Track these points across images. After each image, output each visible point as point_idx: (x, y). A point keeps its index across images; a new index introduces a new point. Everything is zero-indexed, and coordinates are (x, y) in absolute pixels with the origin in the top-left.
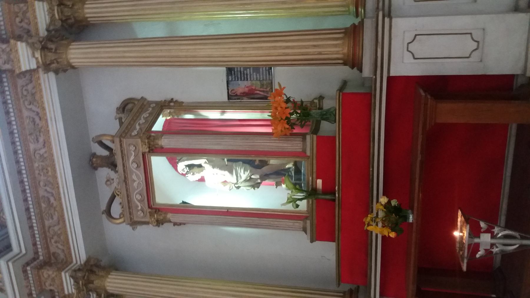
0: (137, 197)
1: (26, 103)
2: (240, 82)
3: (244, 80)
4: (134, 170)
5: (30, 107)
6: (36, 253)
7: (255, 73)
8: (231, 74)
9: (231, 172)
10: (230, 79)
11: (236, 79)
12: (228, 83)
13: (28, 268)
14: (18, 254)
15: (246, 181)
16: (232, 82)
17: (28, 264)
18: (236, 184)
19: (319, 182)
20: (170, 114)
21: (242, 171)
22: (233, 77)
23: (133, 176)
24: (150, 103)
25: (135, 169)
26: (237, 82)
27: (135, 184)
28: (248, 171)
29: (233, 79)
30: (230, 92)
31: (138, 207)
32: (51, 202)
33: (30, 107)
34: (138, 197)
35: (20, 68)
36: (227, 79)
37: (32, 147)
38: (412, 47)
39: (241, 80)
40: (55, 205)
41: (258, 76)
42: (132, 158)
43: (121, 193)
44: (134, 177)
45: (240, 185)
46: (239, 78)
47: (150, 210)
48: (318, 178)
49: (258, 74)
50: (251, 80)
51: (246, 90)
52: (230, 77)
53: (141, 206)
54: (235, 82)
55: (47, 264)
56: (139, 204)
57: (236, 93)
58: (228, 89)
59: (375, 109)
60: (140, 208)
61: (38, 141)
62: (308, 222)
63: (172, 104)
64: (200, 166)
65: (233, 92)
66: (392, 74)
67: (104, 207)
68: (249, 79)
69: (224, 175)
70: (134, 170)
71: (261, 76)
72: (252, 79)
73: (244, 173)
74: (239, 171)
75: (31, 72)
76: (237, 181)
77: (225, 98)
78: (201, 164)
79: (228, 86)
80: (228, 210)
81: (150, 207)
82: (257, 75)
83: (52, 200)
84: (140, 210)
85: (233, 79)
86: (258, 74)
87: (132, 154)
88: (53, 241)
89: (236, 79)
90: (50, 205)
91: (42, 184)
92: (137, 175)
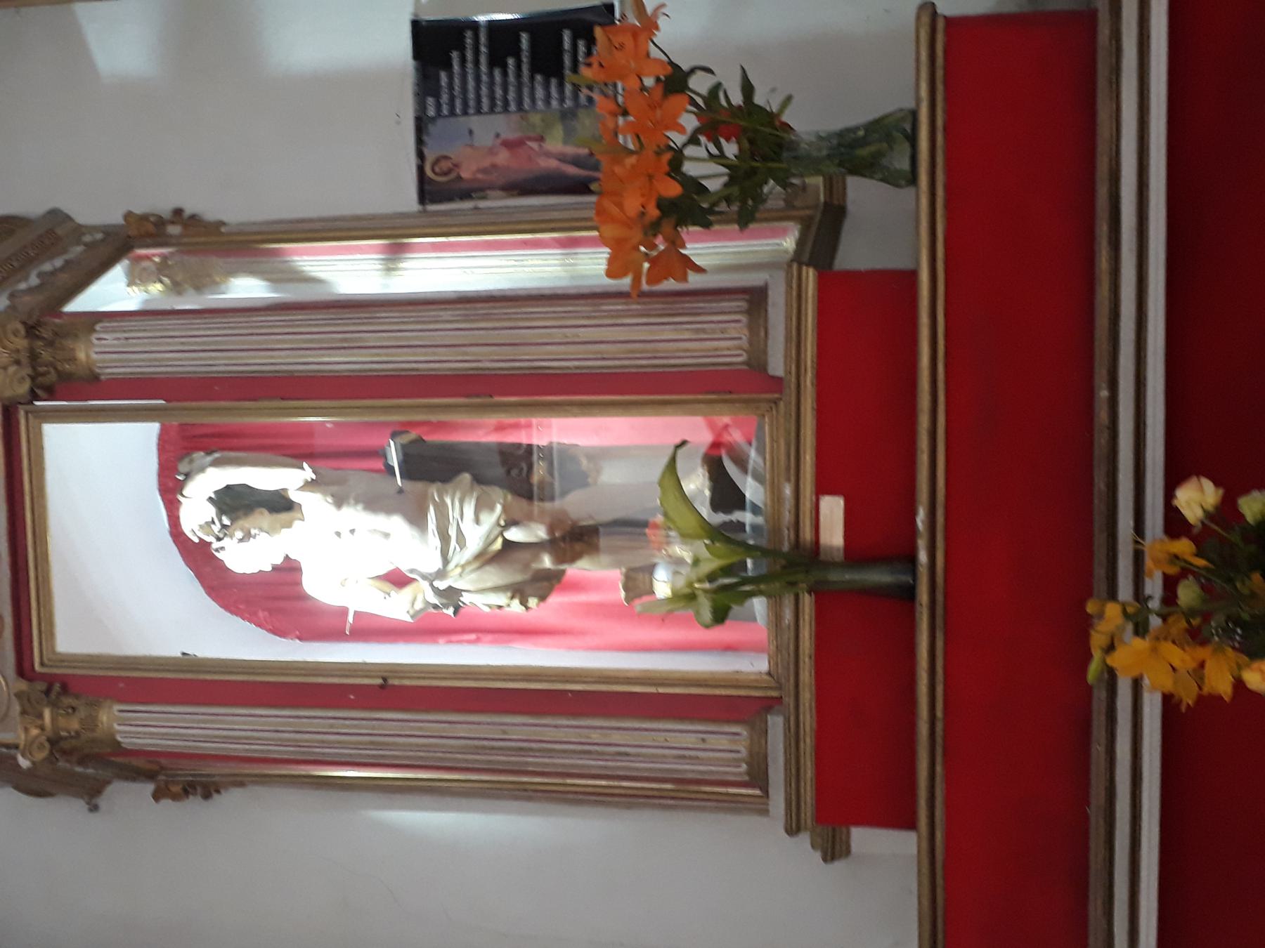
2: (474, 122)
3: (492, 109)
7: (539, 78)
8: (437, 96)
9: (417, 519)
10: (431, 112)
11: (458, 103)
12: (421, 125)
15: (485, 559)
16: (440, 122)
18: (441, 574)
19: (833, 509)
21: (469, 509)
22: (445, 98)
24: (79, 231)
26: (462, 119)
28: (492, 509)
29: (445, 111)
36: (416, 111)
39: (479, 111)
45: (458, 585)
46: (472, 103)
47: (23, 685)
48: (823, 488)
54: (452, 120)
57: (452, 176)
58: (421, 155)
59: (1117, 70)
62: (776, 723)
64: (280, 504)
65: (445, 165)
68: (513, 107)
69: (387, 535)
73: (477, 521)
74: (454, 514)
76: (446, 561)
77: (406, 198)
78: (285, 490)
79: (420, 142)
80: (385, 679)
81: (23, 669)
85: (445, 111)
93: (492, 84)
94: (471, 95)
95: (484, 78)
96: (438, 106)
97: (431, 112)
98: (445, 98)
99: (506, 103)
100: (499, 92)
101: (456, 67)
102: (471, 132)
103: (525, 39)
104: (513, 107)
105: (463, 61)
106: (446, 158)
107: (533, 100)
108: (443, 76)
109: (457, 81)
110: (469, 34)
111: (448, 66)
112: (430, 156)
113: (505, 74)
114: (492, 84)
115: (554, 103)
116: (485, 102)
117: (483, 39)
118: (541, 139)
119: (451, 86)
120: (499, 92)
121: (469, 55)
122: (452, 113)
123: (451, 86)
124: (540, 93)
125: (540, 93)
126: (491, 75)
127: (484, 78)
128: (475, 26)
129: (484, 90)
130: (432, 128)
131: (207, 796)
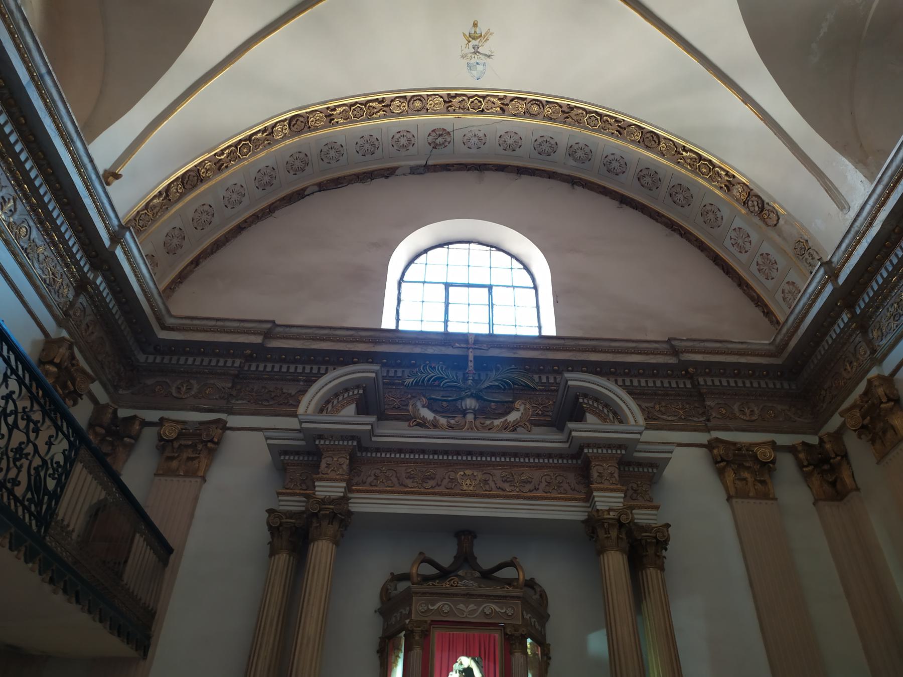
0: (446, 606)
1: (548, 478)
5: (543, 480)
6: (367, 450)
13: (355, 443)
14: (373, 433)
17: (359, 442)
20: (534, 654)
23: (472, 605)
24: (543, 626)
25: (483, 610)
27: (461, 606)
31: (432, 606)
32: (428, 481)
33: (543, 480)
34: (446, 609)
35: (598, 490)
37: (498, 473)
40: (425, 485)
42: (498, 609)
43: (452, 586)
44: (472, 607)
47: (429, 622)
53: (433, 610)
55: (354, 462)
56: (436, 607)
60: (431, 607)
61: (504, 482)
63: (545, 658)
67: (429, 555)
70: (481, 608)
75: (588, 498)
81: (434, 622)
83: (432, 483)
84: (428, 608)
87: (502, 609)
88: (378, 472)
90: (426, 479)
91: (452, 475)
92: (474, 611)
131: (378, 652)
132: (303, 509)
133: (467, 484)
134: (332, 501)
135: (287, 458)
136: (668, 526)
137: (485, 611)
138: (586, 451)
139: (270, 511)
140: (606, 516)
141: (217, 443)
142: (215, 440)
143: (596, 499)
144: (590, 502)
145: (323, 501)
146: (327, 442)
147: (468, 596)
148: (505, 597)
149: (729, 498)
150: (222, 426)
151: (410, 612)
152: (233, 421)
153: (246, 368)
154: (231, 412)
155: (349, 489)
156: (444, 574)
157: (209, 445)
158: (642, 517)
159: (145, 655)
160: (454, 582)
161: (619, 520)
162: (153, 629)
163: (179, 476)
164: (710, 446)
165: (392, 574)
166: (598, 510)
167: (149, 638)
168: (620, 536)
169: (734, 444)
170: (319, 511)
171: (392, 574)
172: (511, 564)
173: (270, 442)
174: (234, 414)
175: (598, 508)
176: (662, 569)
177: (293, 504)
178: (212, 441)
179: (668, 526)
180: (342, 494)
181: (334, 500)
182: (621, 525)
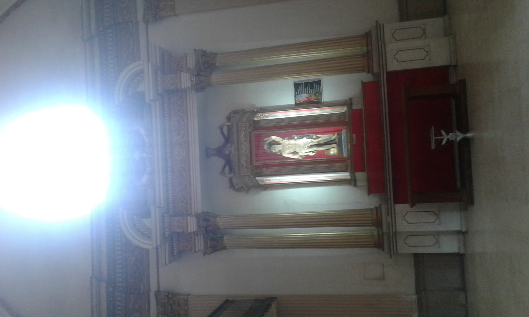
4: (243, 142)
11: (300, 93)
22: (298, 92)
27: (243, 151)
29: (298, 94)
30: (296, 101)
38: (396, 57)
39: (303, 94)
41: (313, 91)
42: (243, 134)
44: (243, 147)
46: (302, 93)
49: (313, 90)
50: (309, 93)
51: (306, 99)
52: (296, 93)
56: (244, 163)
58: (295, 100)
60: (245, 166)
63: (261, 111)
65: (299, 101)
66: (389, 70)
68: (308, 93)
70: (243, 142)
71: (315, 90)
72: (310, 93)
79: (295, 98)
81: (251, 164)
82: (312, 90)
85: (298, 94)
86: (313, 90)
89: (300, 93)
93: (305, 90)
94: (302, 92)
95: (304, 90)
96: (297, 93)
97: (297, 94)
98: (298, 92)
99: (307, 93)
100: (306, 91)
101: (300, 88)
102: (302, 96)
103: (309, 85)
104: (308, 93)
105: (301, 88)
106: (298, 100)
107: (310, 92)
108: (298, 90)
109: (300, 90)
110: (302, 84)
111: (299, 88)
112: (297, 100)
113: (306, 89)
114: (305, 90)
115: (313, 92)
116: (304, 93)
117: (303, 85)
118: (312, 97)
119: (299, 91)
120: (306, 91)
121: (302, 87)
122: (299, 94)
123: (299, 91)
124: (311, 91)
125: (311, 91)
126: (305, 89)
127: (304, 90)
128: (302, 83)
129: (304, 91)
130: (297, 96)
132: (202, 236)
133: (183, 154)
134: (198, 222)
135: (175, 252)
136: (195, 50)
137: (244, 140)
138: (160, 92)
139: (205, 254)
140: (195, 82)
141: (169, 293)
142: (167, 294)
143: (186, 87)
144: (187, 89)
145: (199, 226)
146: (167, 230)
147: (238, 149)
148: (237, 131)
149: (176, 15)
150: (158, 293)
151: (247, 176)
152: (154, 288)
153: (121, 289)
154: (149, 291)
155: (191, 215)
156: (228, 162)
157: (170, 296)
158: (191, 63)
159: (275, 298)
160: (233, 156)
161: (196, 76)
162: (263, 298)
163: (188, 308)
164: (147, 22)
165: (230, 188)
166: (192, 86)
167: (268, 299)
168: (204, 75)
169: (145, 9)
170: (204, 227)
171: (230, 188)
172: (221, 129)
173: (167, 262)
174: (150, 289)
175: (190, 85)
176: (216, 54)
177: (200, 243)
178: (167, 296)
179: (195, 50)
180: (194, 218)
181: (198, 221)
182: (198, 75)
